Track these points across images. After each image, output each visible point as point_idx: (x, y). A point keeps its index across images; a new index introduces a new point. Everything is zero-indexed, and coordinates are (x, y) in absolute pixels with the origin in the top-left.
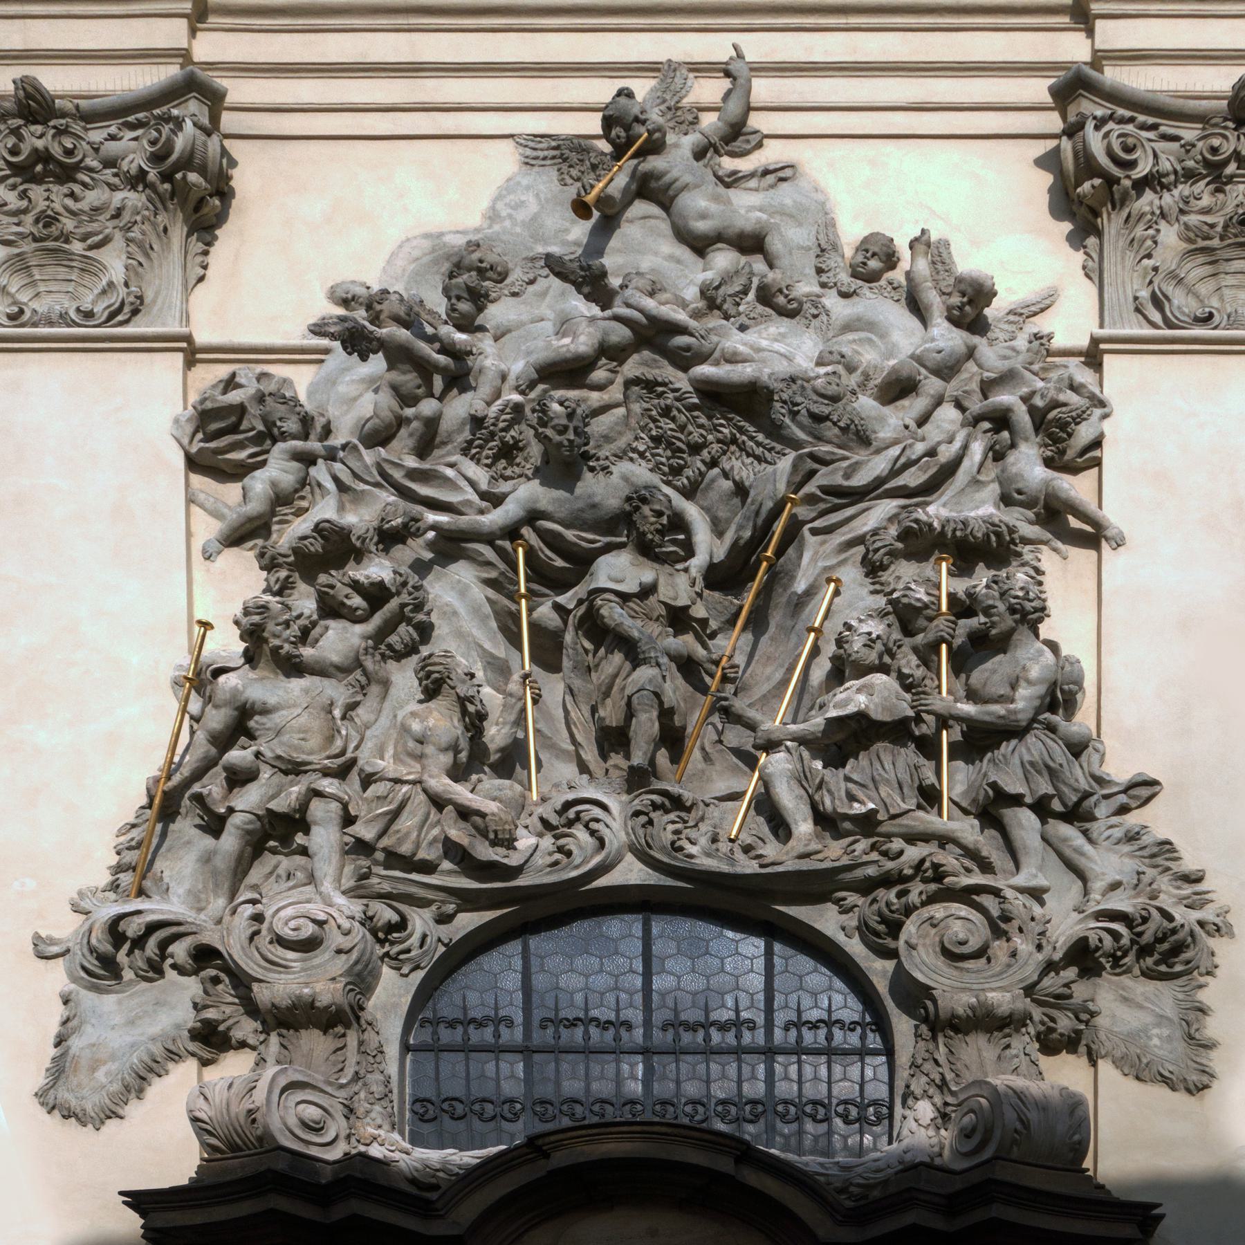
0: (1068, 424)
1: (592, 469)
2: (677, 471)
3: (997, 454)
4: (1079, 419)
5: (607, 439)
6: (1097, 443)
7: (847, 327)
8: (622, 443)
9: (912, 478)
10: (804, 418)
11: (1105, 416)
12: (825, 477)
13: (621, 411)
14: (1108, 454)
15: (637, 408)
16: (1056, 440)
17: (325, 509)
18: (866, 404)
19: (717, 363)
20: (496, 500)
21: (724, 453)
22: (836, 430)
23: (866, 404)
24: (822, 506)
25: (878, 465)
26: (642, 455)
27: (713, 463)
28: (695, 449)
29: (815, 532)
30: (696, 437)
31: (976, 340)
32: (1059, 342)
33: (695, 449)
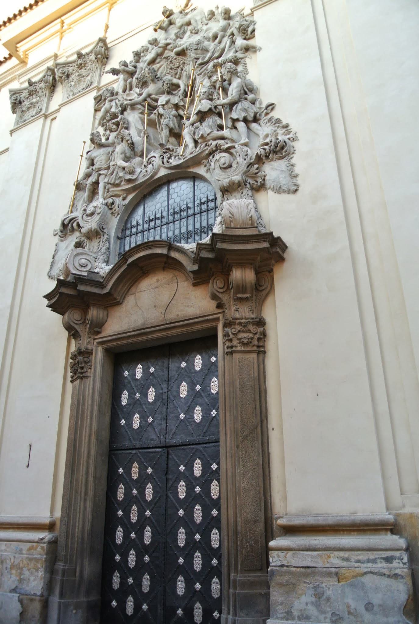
0: (246, 29)
1: (158, 80)
2: (176, 74)
3: (233, 42)
4: (248, 26)
5: (162, 73)
6: (254, 31)
7: (206, 31)
8: (164, 73)
9: (216, 55)
10: (193, 51)
11: (255, 24)
12: (200, 61)
13: (163, 67)
14: (256, 32)
15: (165, 64)
16: (244, 33)
17: (113, 110)
18: (206, 43)
19: (178, 47)
20: (140, 95)
21: (184, 66)
22: (200, 51)
23: (206, 43)
24: (200, 68)
25: (209, 55)
26: (169, 73)
27: (182, 70)
28: (178, 67)
29: (199, 75)
30: (178, 65)
31: (229, 21)
32: (245, 14)
33: (178, 67)
